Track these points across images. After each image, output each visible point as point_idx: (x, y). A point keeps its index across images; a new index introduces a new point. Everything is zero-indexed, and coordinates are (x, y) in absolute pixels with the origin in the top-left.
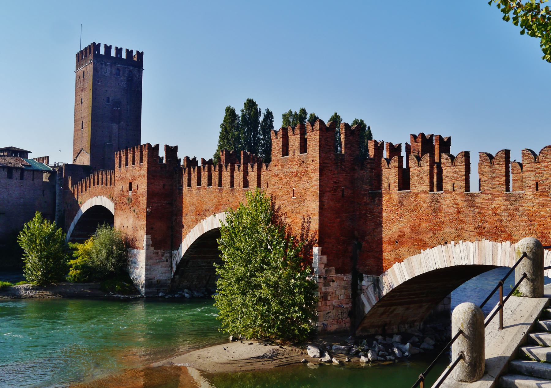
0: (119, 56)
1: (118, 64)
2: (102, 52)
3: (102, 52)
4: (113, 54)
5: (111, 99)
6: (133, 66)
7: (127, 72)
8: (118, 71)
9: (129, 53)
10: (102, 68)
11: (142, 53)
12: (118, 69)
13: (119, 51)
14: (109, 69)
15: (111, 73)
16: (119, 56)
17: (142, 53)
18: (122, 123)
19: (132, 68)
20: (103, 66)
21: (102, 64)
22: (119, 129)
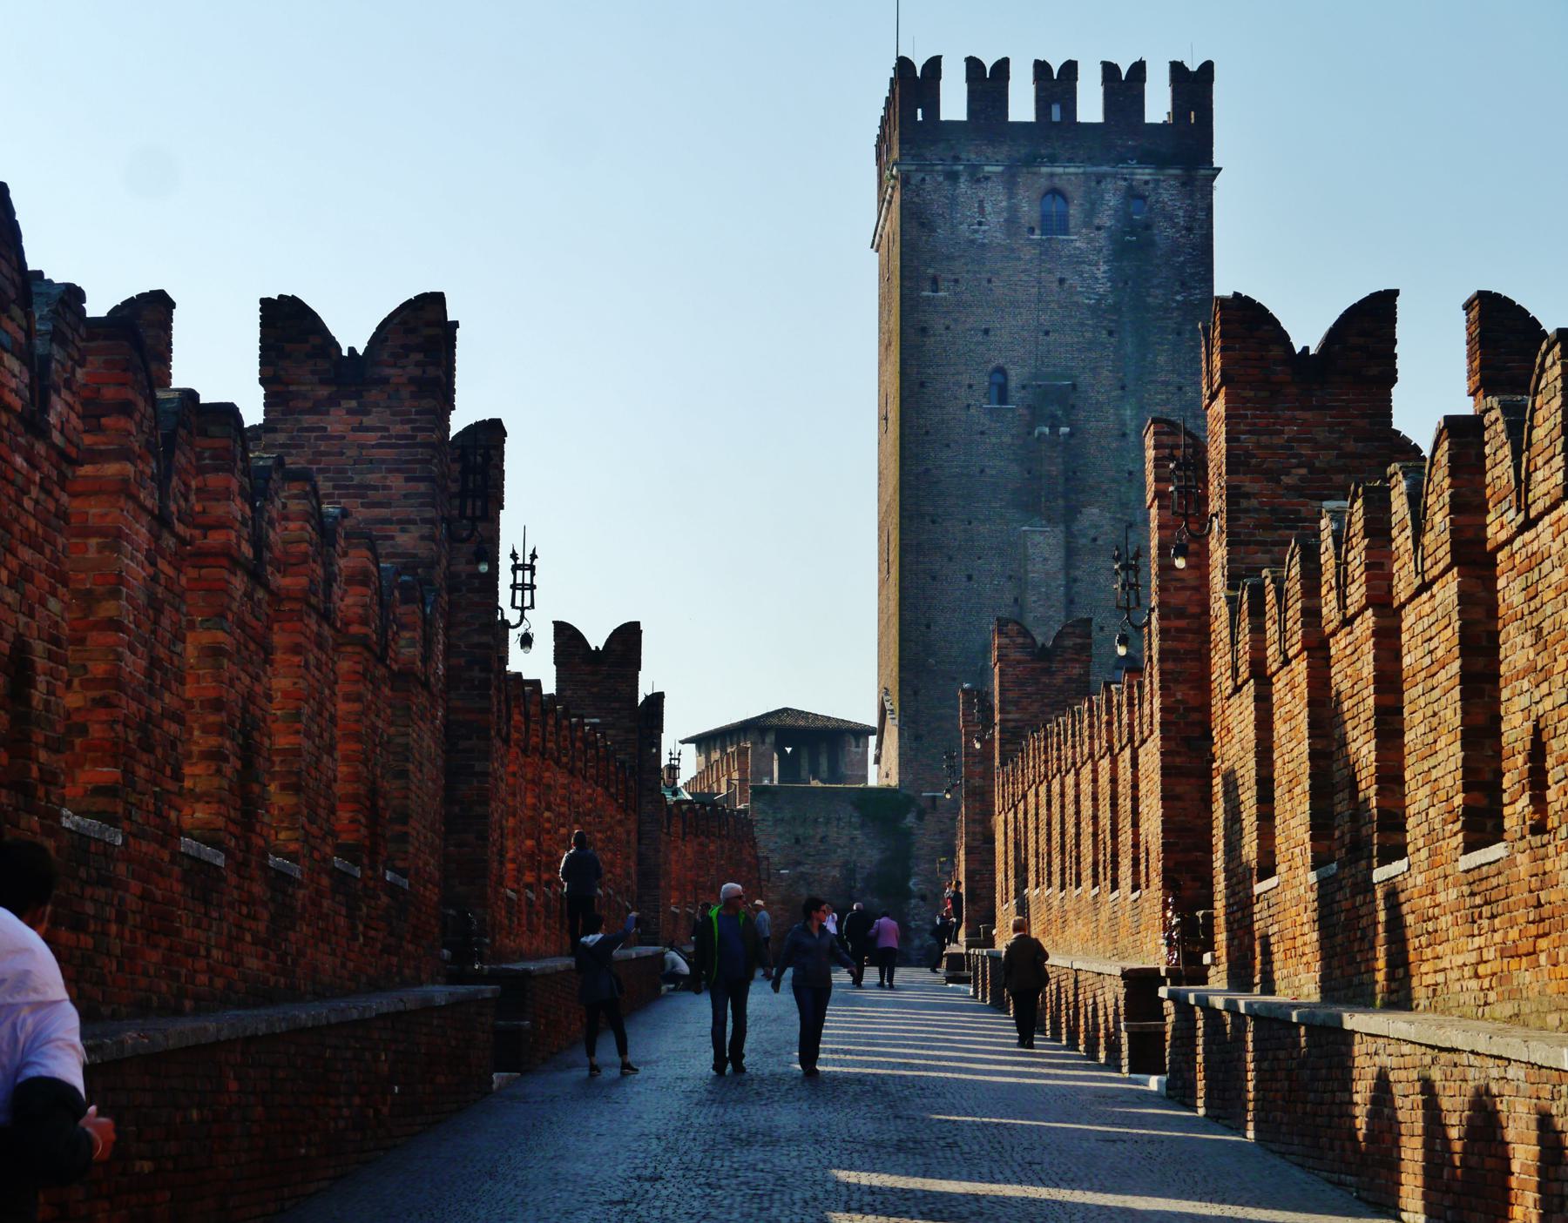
0: (1056, 114)
1: (1053, 160)
2: (954, 104)
3: (954, 104)
4: (1022, 105)
5: (1016, 376)
6: (1145, 159)
7: (1112, 200)
8: (1055, 206)
9: (1124, 86)
10: (953, 200)
11: (1208, 67)
12: (1055, 192)
13: (1056, 84)
14: (995, 199)
15: (1012, 222)
16: (1056, 114)
17: (1208, 67)
18: (1092, 515)
19: (1144, 174)
20: (963, 186)
21: (953, 177)
22: (1071, 553)
